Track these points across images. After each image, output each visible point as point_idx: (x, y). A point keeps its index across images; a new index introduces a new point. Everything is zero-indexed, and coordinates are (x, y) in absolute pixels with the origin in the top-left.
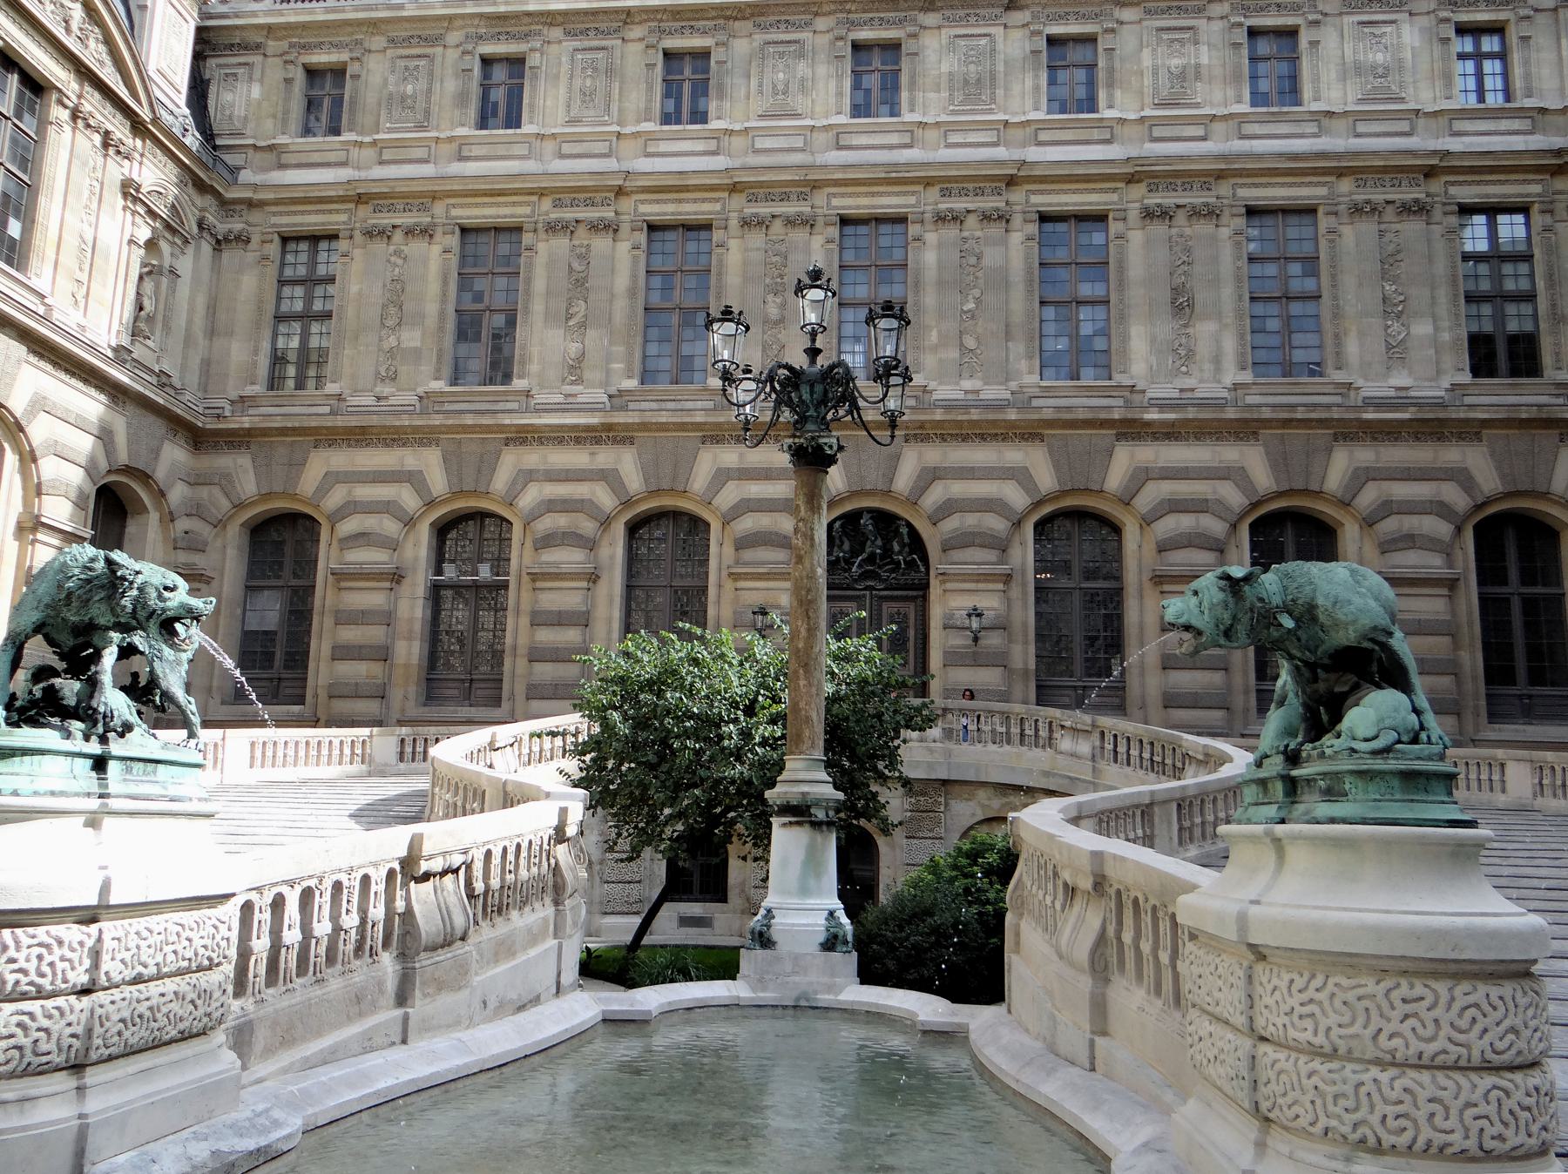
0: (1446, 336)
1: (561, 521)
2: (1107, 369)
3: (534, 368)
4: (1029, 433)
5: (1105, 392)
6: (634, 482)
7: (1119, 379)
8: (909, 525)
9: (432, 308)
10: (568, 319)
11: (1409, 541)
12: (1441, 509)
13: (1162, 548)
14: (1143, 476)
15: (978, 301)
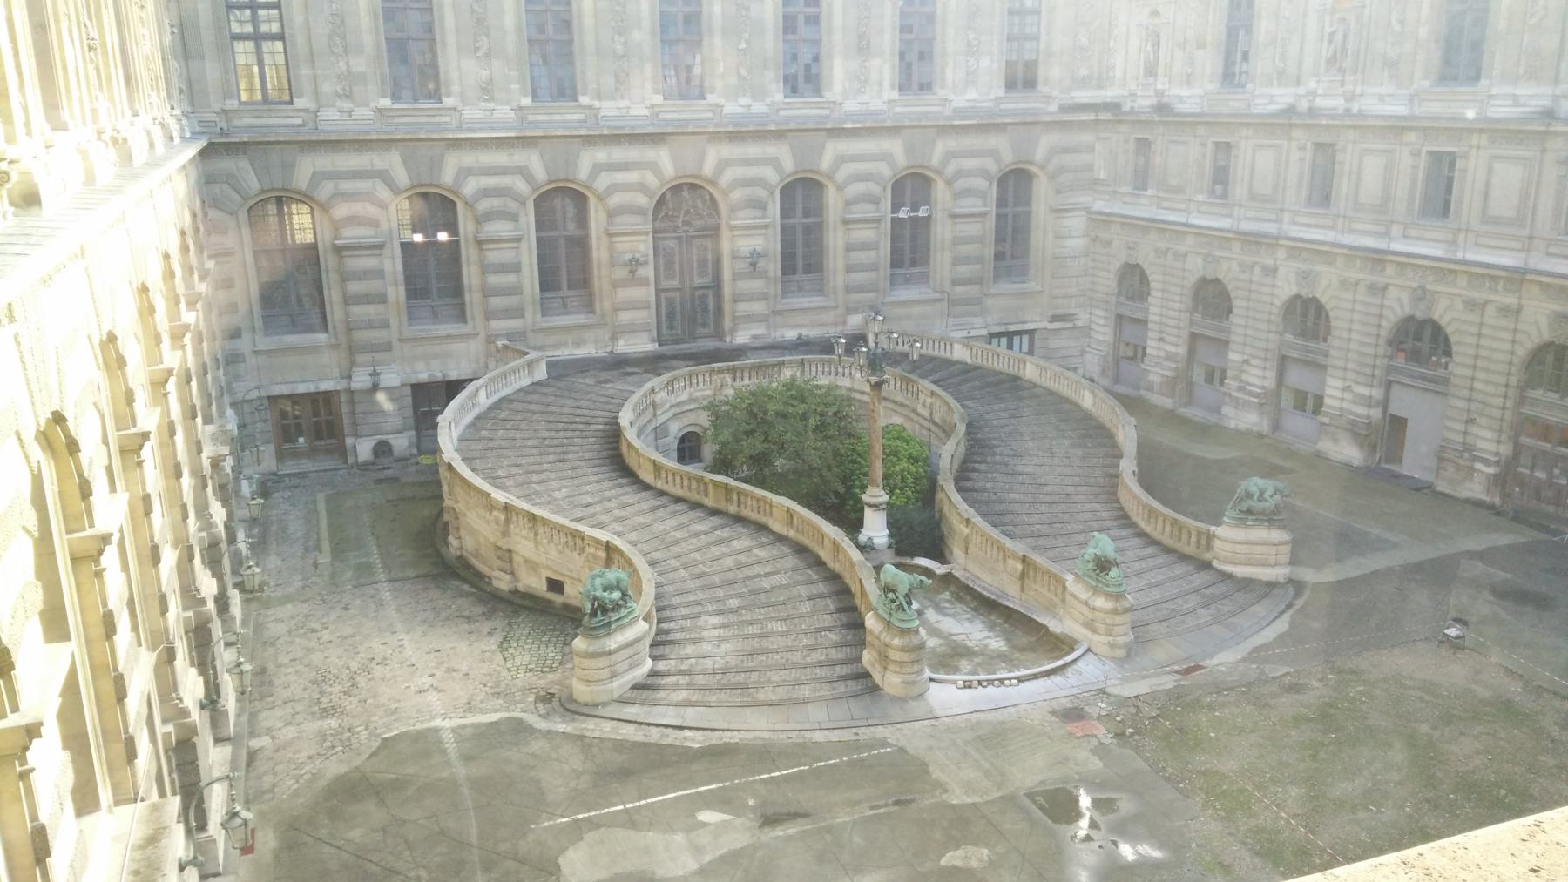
0: (995, 65)
1: (495, 203)
2: (818, 91)
3: (456, 88)
4: (779, 135)
5: (818, 106)
6: (540, 175)
7: (828, 96)
8: (711, 196)
9: (368, 39)
10: (477, 49)
11: (967, 192)
12: (984, 173)
13: (848, 204)
14: (841, 160)
15: (747, 42)
